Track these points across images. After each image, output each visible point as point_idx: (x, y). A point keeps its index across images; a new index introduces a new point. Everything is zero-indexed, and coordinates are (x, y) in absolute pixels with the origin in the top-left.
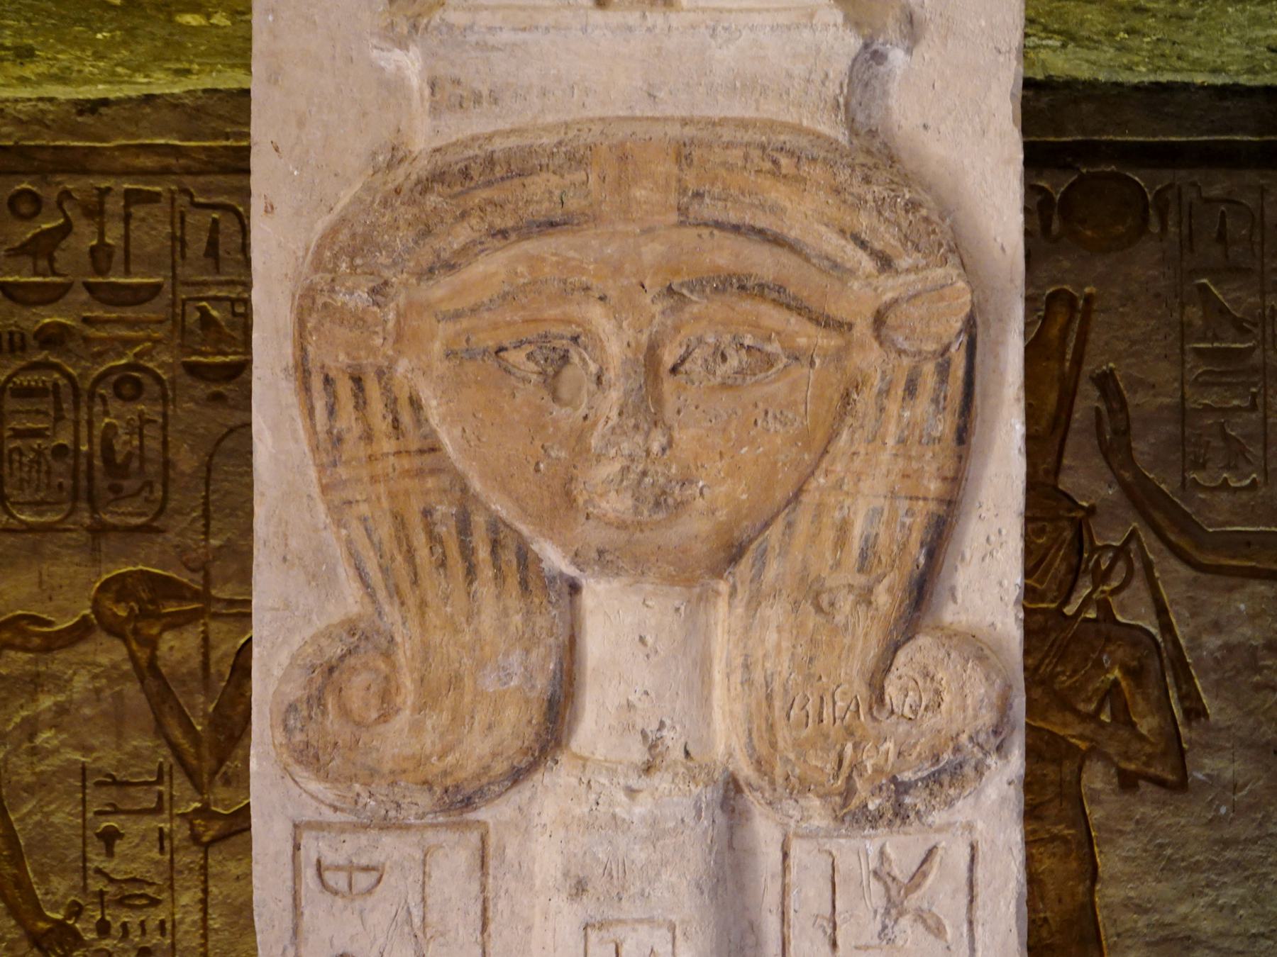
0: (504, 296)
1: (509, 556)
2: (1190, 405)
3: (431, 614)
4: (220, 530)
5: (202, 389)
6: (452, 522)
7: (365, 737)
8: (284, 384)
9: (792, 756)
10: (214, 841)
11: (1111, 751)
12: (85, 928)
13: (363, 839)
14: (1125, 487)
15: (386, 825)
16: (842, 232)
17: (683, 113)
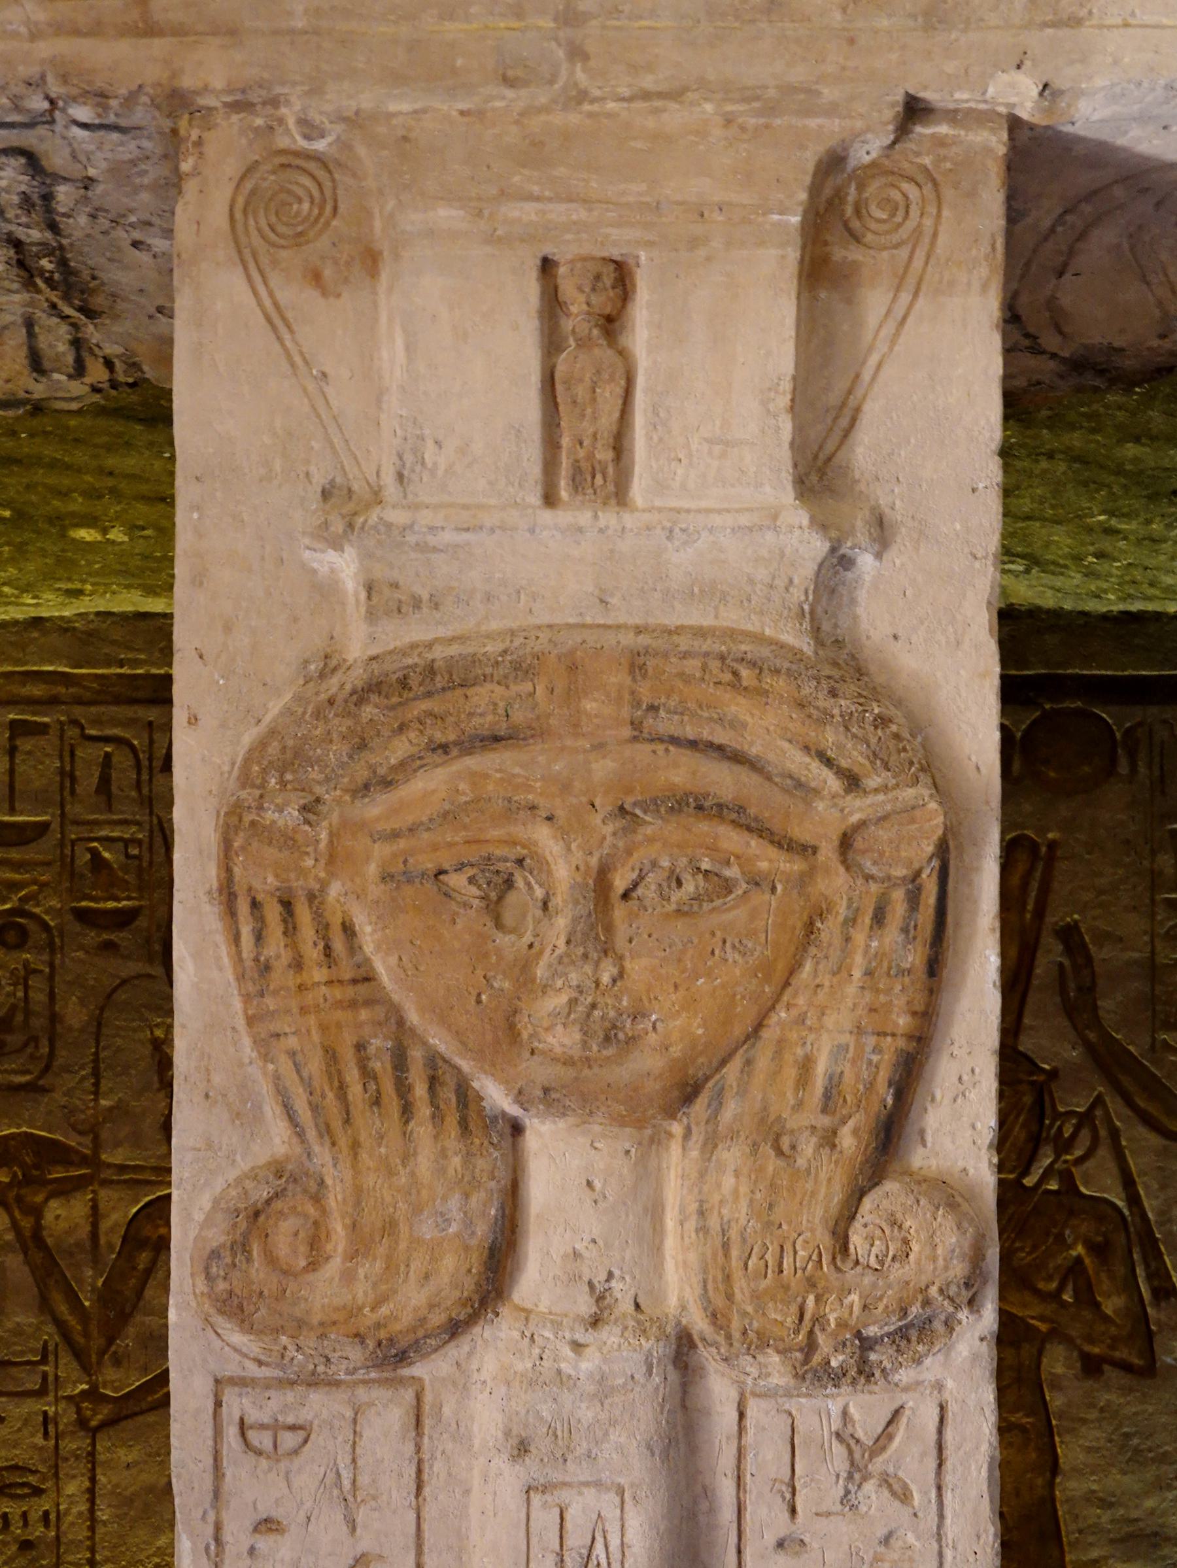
0: (445, 815)
1: (448, 1094)
2: (1161, 959)
3: (364, 1156)
4: (111, 1090)
5: (92, 937)
6: (387, 1058)
7: (292, 1286)
8: (207, 908)
9: (750, 1309)
11: (1073, 1333)
13: (290, 1396)
14: (1090, 1048)
15: (314, 1382)
16: (807, 748)
17: (637, 620)
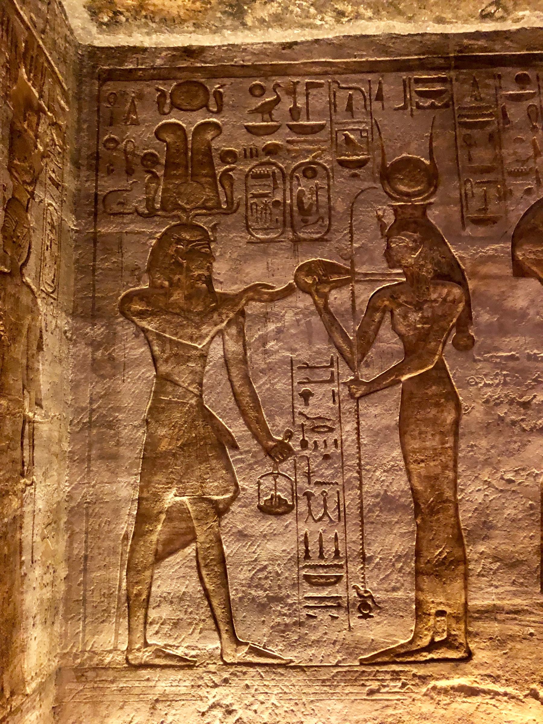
4: (359, 239)
5: (346, 172)
10: (362, 396)
12: (294, 444)
